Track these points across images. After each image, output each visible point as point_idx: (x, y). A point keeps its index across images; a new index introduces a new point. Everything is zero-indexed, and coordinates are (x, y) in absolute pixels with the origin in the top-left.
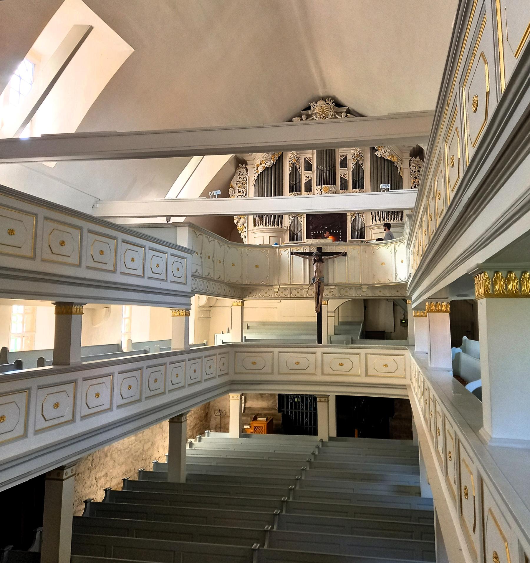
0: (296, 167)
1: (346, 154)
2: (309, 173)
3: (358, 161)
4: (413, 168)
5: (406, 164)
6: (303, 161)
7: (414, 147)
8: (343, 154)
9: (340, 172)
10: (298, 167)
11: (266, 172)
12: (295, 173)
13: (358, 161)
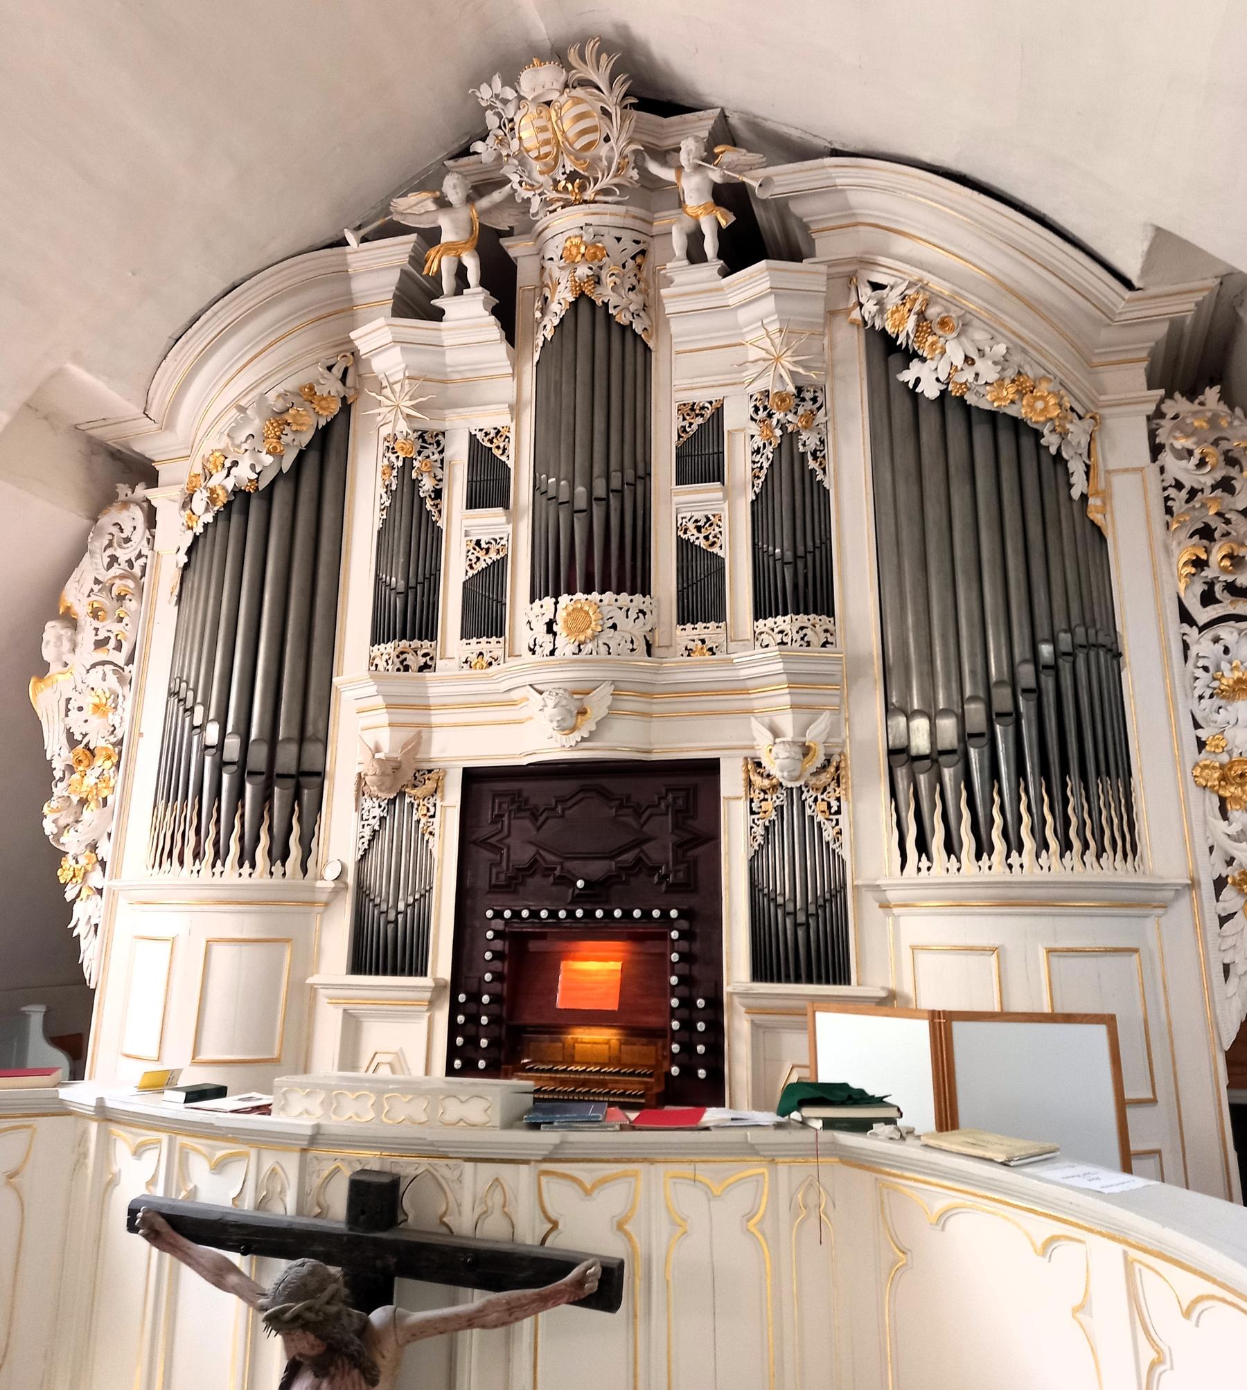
0: (415, 484)
1: (715, 394)
2: (490, 522)
3: (790, 437)
4: (1178, 468)
5: (1126, 441)
6: (458, 452)
7: (1176, 325)
8: (700, 397)
9: (674, 506)
10: (427, 484)
11: (235, 518)
12: (414, 526)
13: (790, 437)
